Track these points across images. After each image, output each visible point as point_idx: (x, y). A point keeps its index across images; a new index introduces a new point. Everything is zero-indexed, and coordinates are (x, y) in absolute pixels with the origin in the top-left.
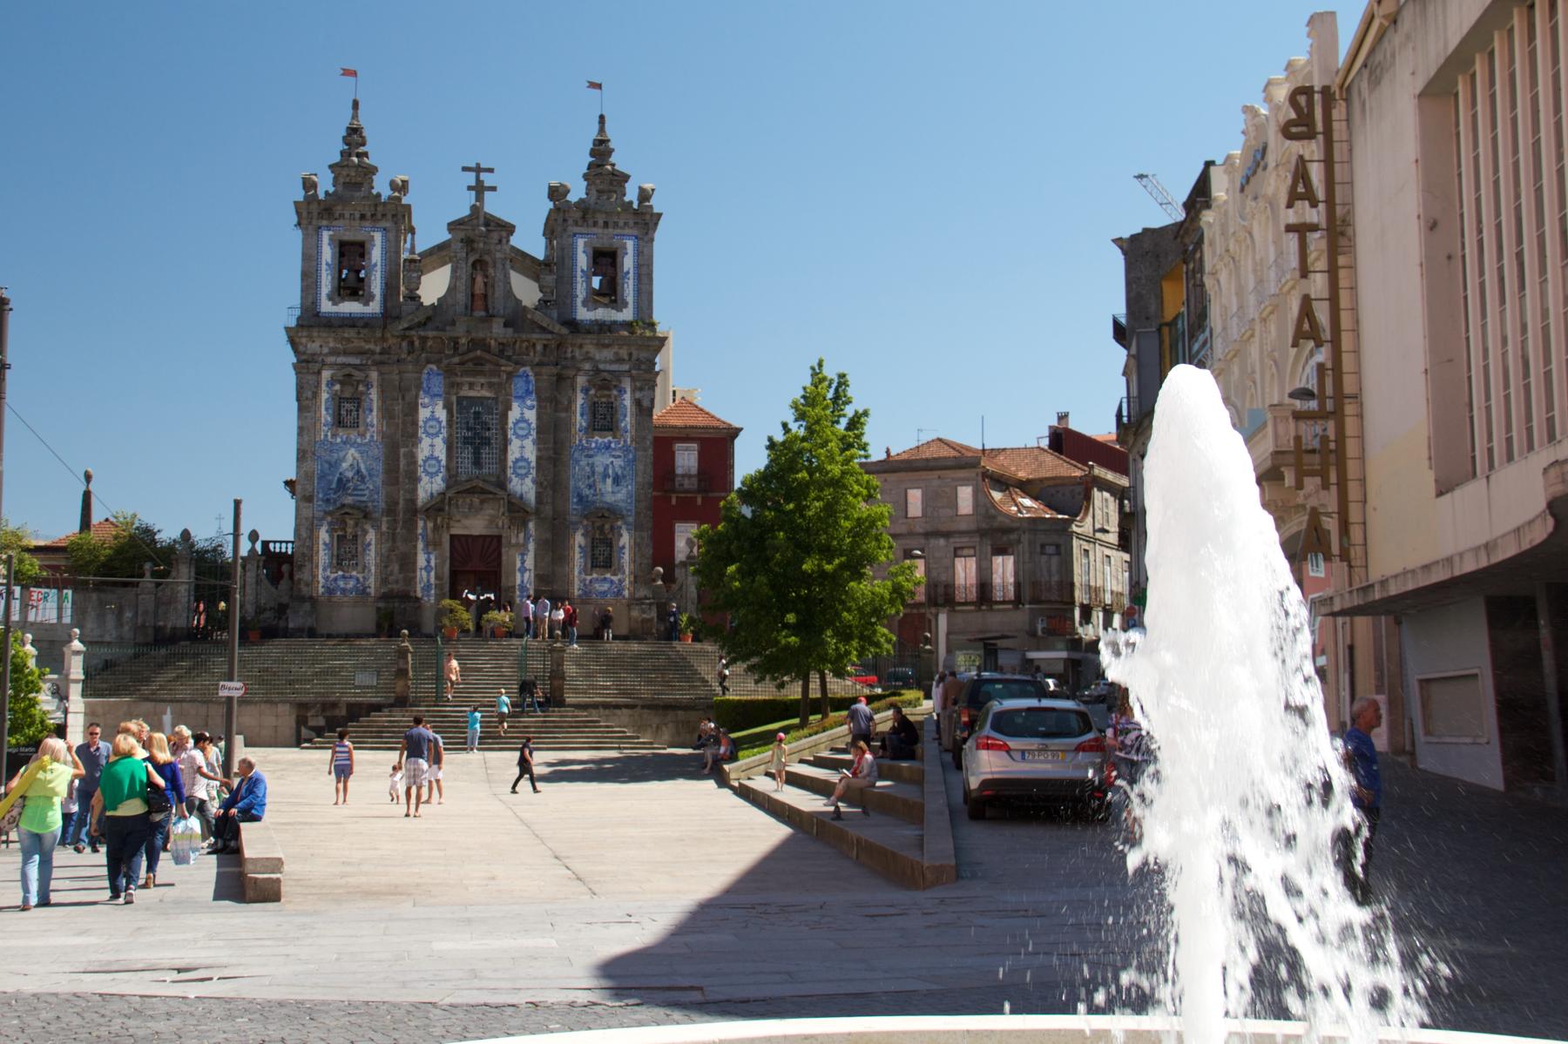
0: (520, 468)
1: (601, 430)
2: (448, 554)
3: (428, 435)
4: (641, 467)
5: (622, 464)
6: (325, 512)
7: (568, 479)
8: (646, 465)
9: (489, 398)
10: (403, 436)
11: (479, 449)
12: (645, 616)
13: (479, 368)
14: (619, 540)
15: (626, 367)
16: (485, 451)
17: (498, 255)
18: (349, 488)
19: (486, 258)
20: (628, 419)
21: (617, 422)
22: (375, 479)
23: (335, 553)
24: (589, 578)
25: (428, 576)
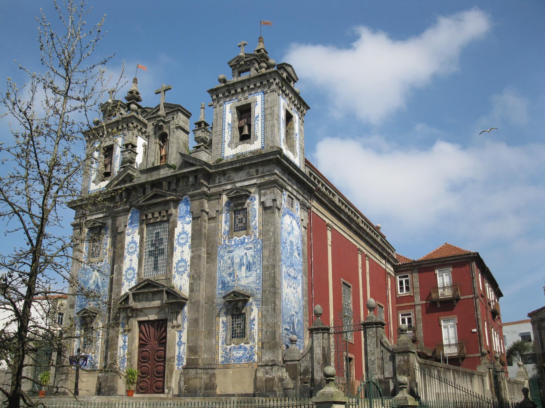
5: (253, 253)
7: (215, 271)
8: (269, 252)
11: (157, 257)
12: (268, 376)
14: (250, 315)
17: (172, 127)
20: (257, 219)
21: (249, 222)
24: (229, 347)
25: (124, 352)
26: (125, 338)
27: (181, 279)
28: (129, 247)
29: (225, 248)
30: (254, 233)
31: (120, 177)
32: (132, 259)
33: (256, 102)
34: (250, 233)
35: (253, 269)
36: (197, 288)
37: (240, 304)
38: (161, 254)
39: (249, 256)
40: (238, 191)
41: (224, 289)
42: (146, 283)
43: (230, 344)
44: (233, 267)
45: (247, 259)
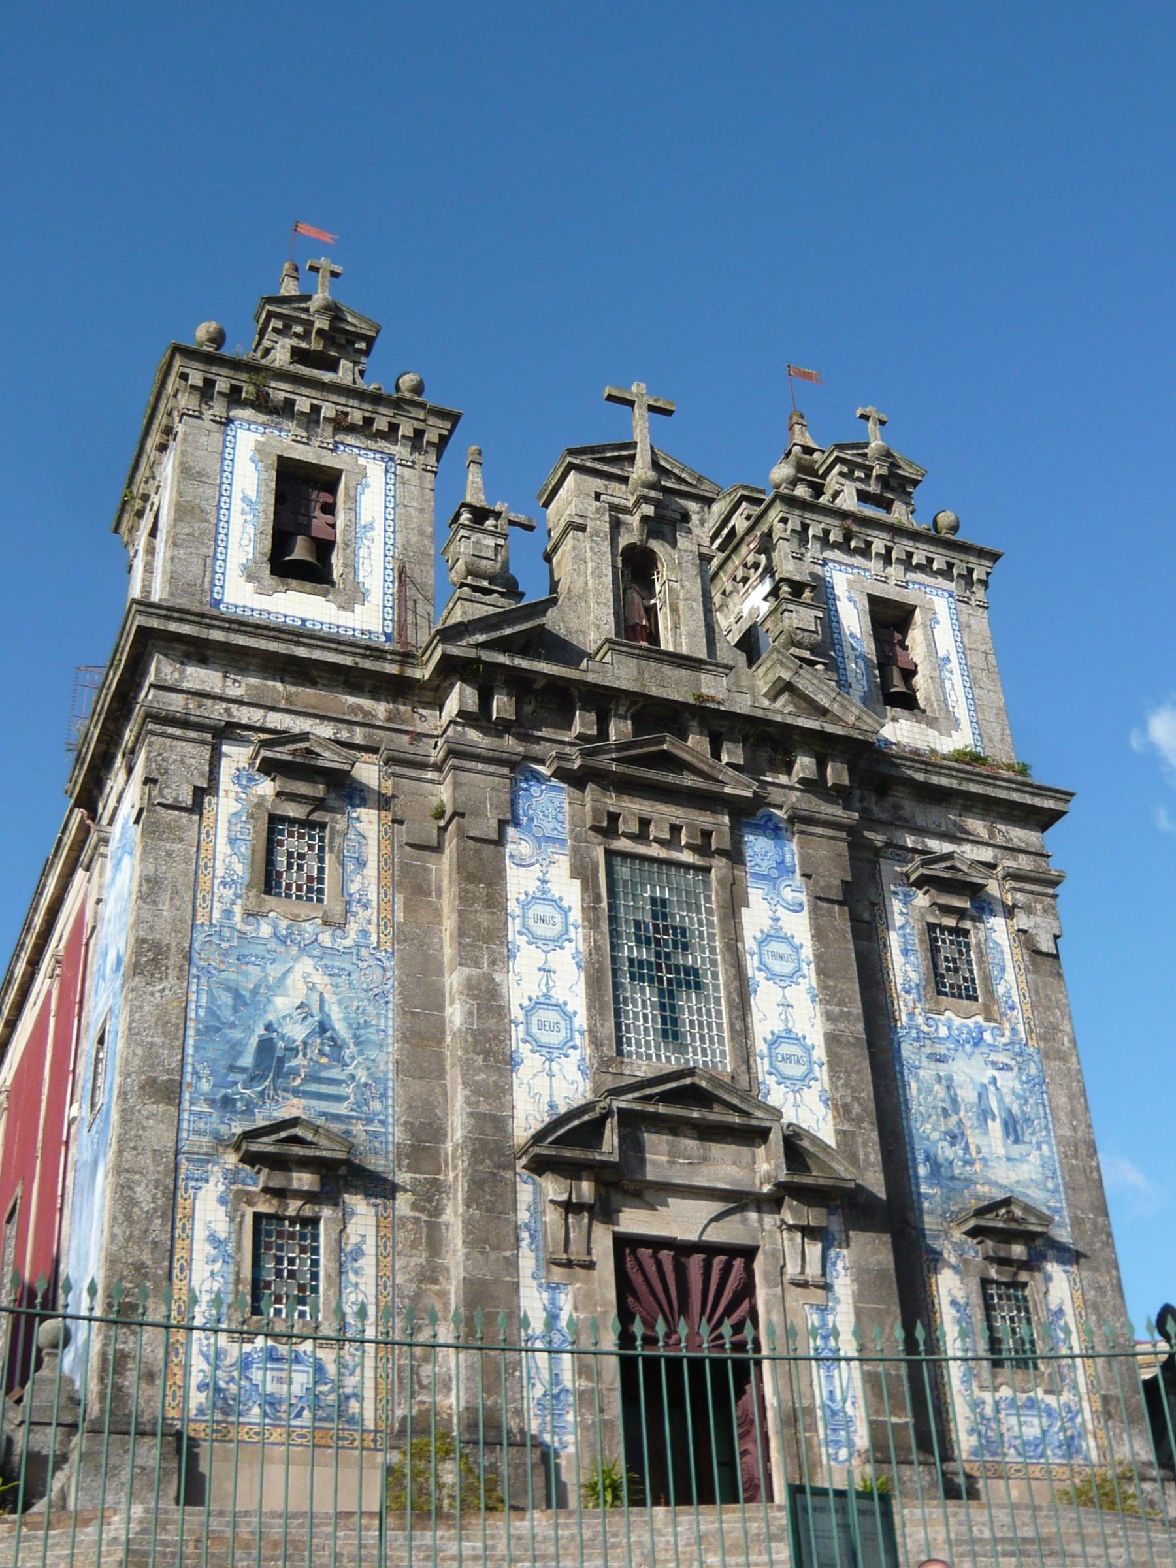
0: (787, 1059)
1: (953, 995)
2: (612, 1295)
3: (534, 940)
4: (1063, 1100)
5: (1018, 1086)
6: (219, 1139)
8: (1071, 1098)
9: (687, 867)
10: (461, 932)
11: (671, 995)
13: (670, 778)
15: (986, 855)
16: (688, 1002)
18: (295, 1072)
19: (655, 545)
20: (1010, 976)
21: (987, 978)
22: (373, 1053)
23: (247, 1272)
26: (553, 1301)
27: (796, 1106)
28: (530, 914)
29: (918, 1039)
30: (1009, 1020)
31: (511, 623)
32: (553, 967)
33: (935, 613)
34: (997, 1017)
35: (1027, 1139)
36: (867, 1155)
37: (1018, 1250)
38: (688, 986)
39: (1004, 1090)
40: (958, 865)
41: (938, 1184)
42: (688, 1081)
43: (996, 1389)
44: (957, 1112)
45: (1001, 1100)
